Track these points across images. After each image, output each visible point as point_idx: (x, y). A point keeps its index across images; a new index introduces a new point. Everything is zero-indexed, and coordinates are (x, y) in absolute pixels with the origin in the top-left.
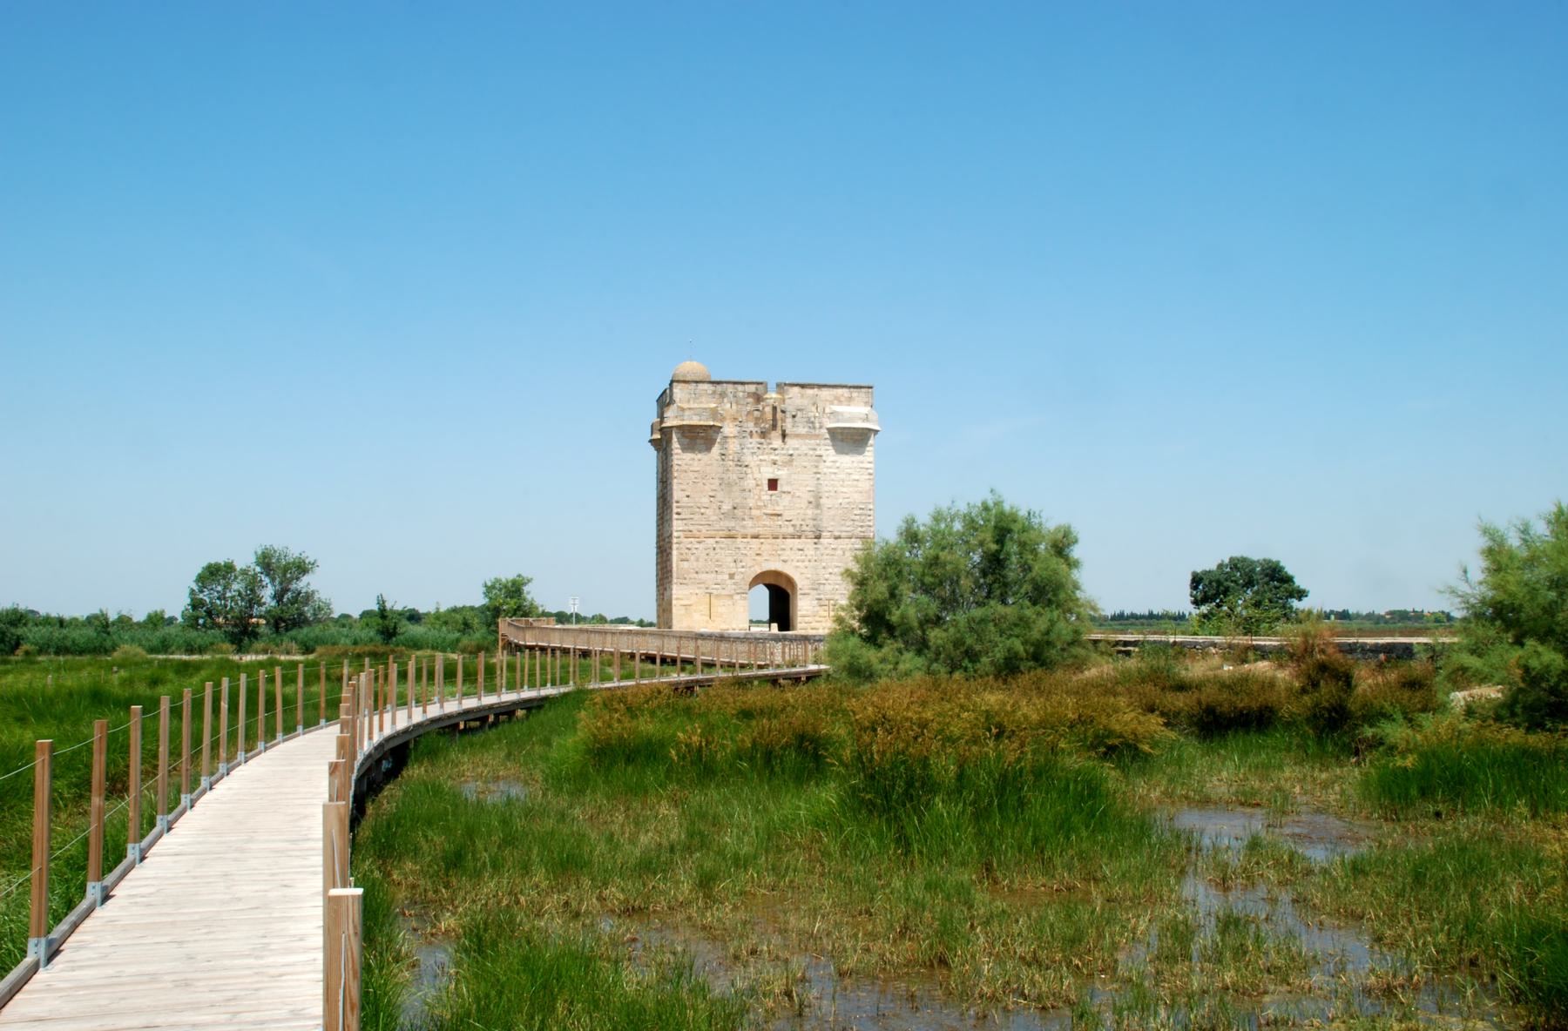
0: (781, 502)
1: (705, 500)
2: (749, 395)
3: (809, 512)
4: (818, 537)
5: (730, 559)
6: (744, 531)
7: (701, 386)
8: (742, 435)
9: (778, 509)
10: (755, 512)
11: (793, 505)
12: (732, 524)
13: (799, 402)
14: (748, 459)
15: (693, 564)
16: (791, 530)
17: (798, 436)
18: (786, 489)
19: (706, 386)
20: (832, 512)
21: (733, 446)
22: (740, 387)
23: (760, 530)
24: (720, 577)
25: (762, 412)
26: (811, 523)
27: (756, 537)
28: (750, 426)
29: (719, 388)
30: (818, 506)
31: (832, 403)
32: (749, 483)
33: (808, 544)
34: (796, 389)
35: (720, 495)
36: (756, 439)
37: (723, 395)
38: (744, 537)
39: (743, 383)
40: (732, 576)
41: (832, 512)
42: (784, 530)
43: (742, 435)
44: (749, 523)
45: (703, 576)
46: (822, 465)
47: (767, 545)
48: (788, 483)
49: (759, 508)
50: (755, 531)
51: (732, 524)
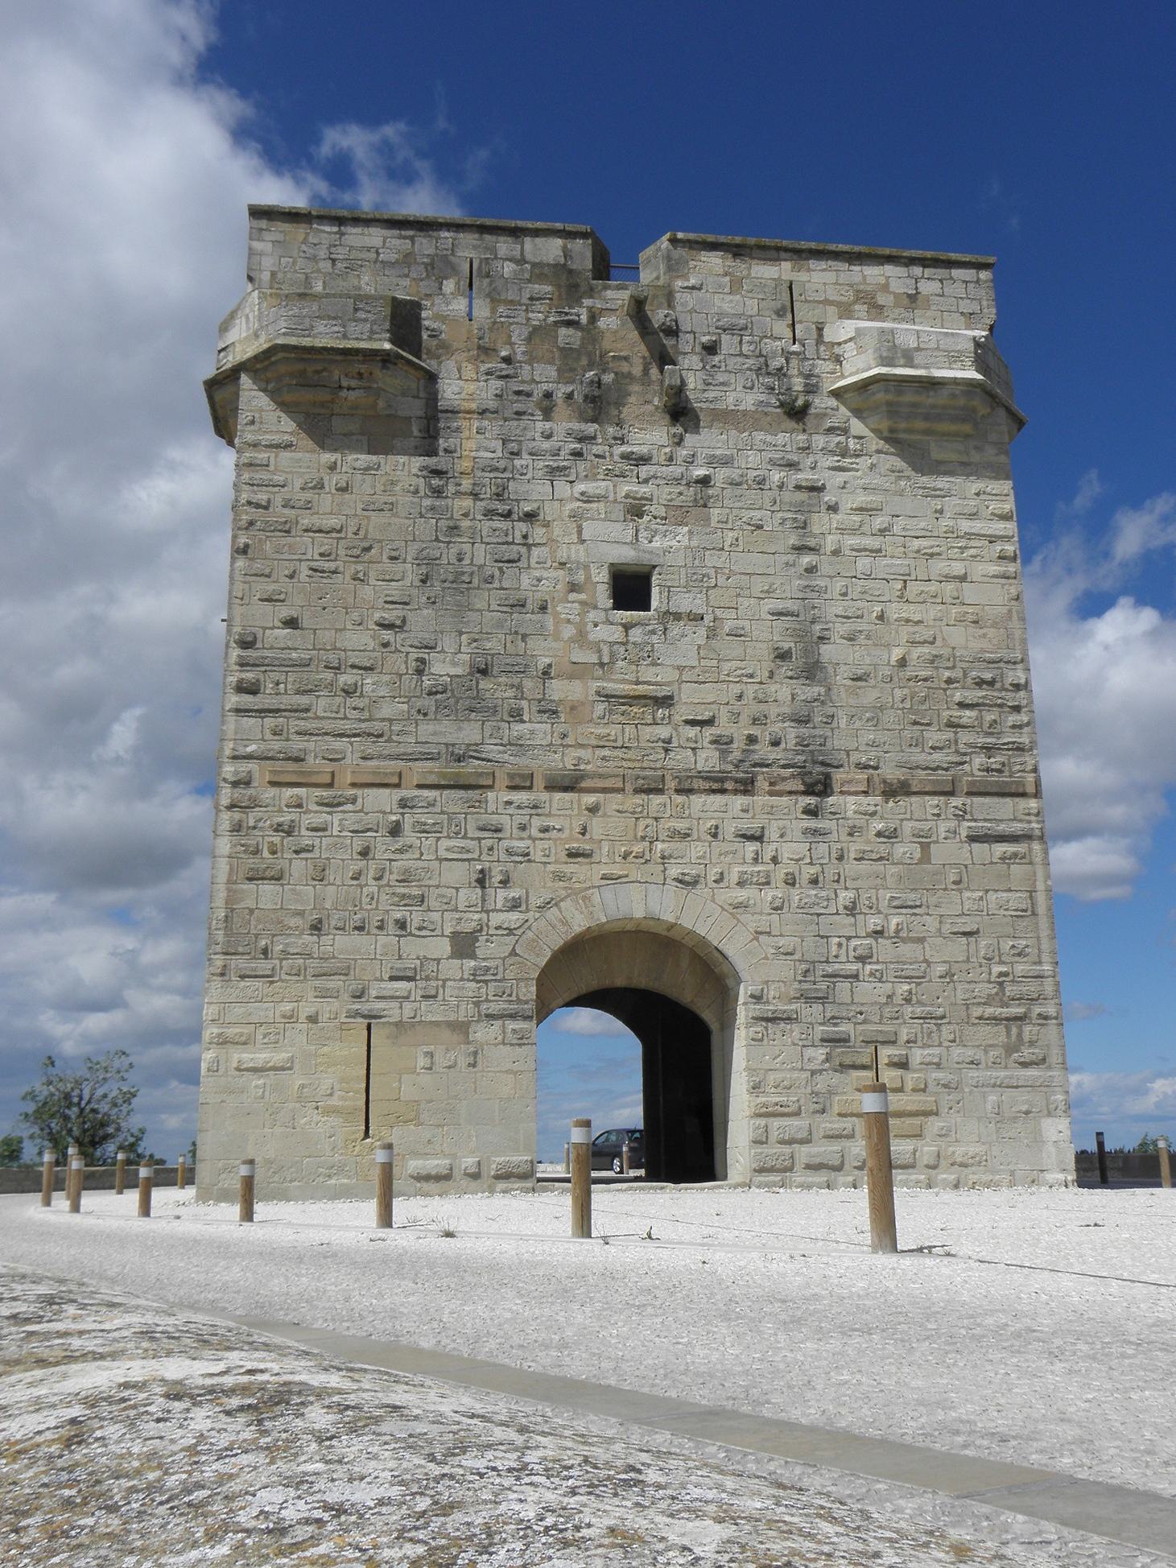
0: (674, 658)
1: (360, 641)
2: (539, 272)
3: (782, 690)
4: (820, 787)
5: (458, 874)
6: (525, 762)
7: (356, 236)
8: (514, 404)
9: (657, 677)
10: (558, 689)
11: (713, 666)
12: (469, 733)
13: (727, 304)
14: (533, 491)
15: (300, 893)
16: (708, 759)
17: (727, 418)
18: (685, 602)
19: (375, 236)
20: (869, 696)
21: (473, 445)
22: (505, 246)
23: (591, 761)
24: (414, 948)
25: (590, 329)
26: (791, 734)
27: (569, 784)
28: (544, 375)
29: (425, 246)
30: (812, 671)
31: (846, 312)
32: (538, 578)
33: (780, 814)
34: (714, 261)
35: (422, 621)
36: (564, 424)
37: (440, 268)
38: (521, 782)
39: (516, 233)
40: (464, 945)
41: (869, 696)
42: (682, 759)
43: (514, 404)
44: (535, 730)
45: (340, 944)
46: (821, 522)
47: (614, 822)
48: (699, 582)
49: (578, 672)
50: (565, 761)
51: (469, 733)
